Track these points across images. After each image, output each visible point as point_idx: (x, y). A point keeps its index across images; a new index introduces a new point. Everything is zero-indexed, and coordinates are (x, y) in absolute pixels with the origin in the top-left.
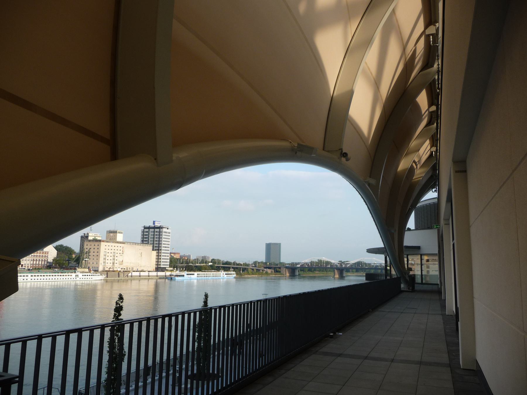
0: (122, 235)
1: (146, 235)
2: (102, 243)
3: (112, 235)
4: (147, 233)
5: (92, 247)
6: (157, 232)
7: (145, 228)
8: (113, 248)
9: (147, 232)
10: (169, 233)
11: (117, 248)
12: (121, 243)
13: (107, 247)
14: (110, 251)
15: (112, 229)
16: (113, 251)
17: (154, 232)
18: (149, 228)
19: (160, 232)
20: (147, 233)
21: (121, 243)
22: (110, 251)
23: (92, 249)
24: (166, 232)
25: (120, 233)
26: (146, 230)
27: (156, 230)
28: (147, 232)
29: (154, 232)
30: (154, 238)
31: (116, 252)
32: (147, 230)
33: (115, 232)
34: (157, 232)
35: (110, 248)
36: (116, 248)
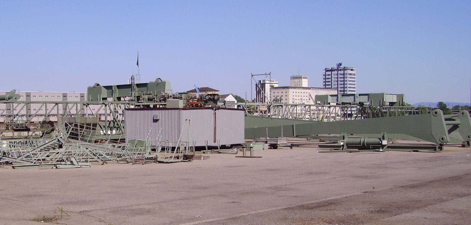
0: (307, 80)
1: (328, 78)
2: (290, 90)
3: (296, 80)
4: (330, 77)
5: (284, 94)
6: (341, 74)
7: (327, 70)
8: (300, 94)
9: (329, 75)
10: (354, 75)
11: (304, 94)
12: (306, 88)
13: (295, 94)
14: (297, 98)
15: (296, 75)
16: (300, 98)
17: (337, 74)
18: (332, 70)
19: (344, 74)
20: (330, 77)
21: (306, 88)
22: (297, 98)
23: (284, 96)
24: (350, 74)
25: (304, 78)
26: (327, 73)
27: (340, 72)
28: (329, 75)
29: (337, 74)
30: (337, 81)
31: (303, 98)
32: (330, 73)
33: (300, 78)
34: (341, 74)
35: (297, 94)
36: (303, 94)
